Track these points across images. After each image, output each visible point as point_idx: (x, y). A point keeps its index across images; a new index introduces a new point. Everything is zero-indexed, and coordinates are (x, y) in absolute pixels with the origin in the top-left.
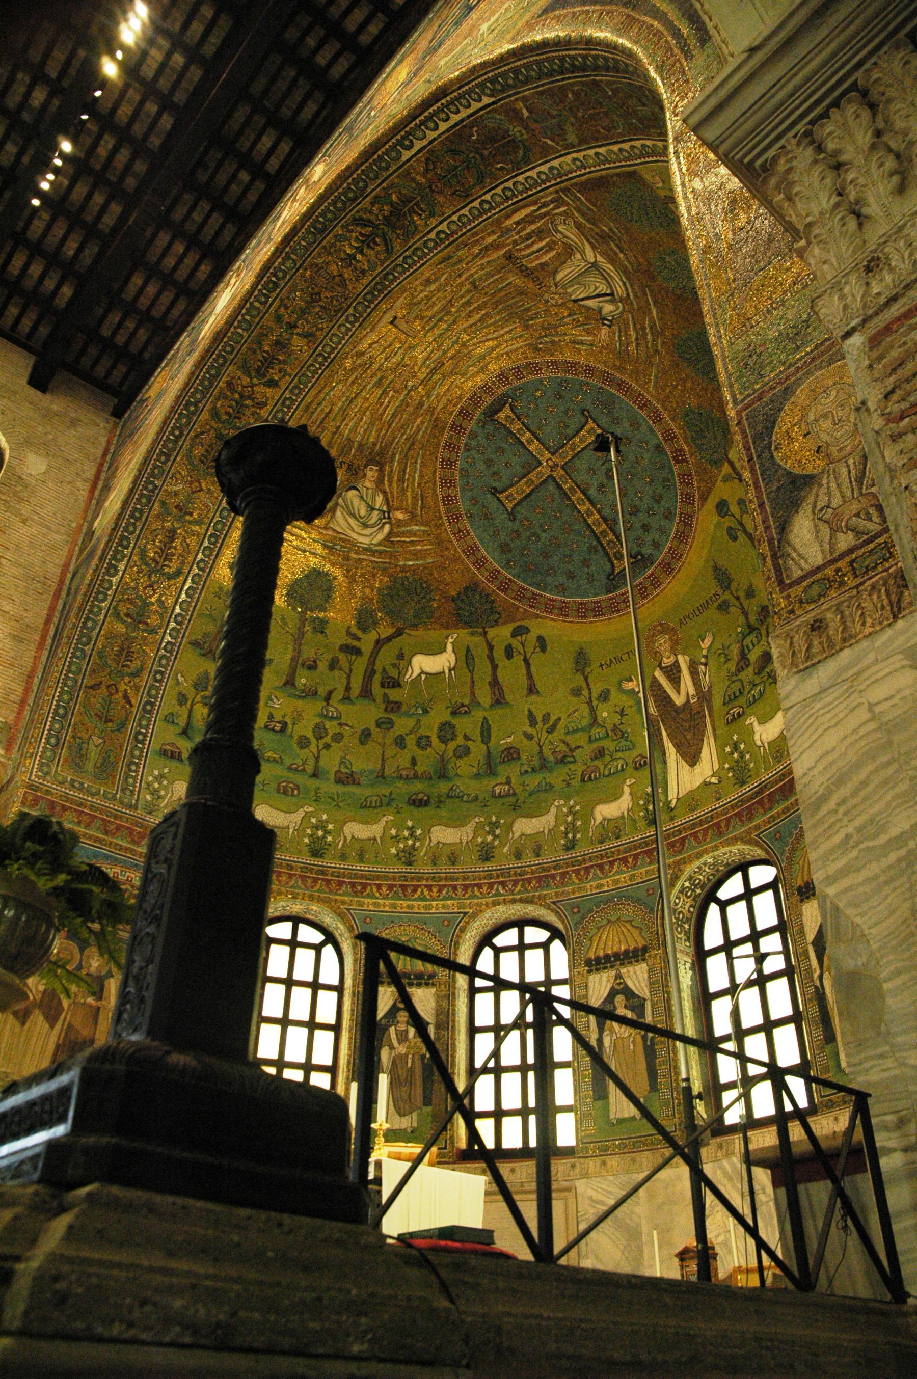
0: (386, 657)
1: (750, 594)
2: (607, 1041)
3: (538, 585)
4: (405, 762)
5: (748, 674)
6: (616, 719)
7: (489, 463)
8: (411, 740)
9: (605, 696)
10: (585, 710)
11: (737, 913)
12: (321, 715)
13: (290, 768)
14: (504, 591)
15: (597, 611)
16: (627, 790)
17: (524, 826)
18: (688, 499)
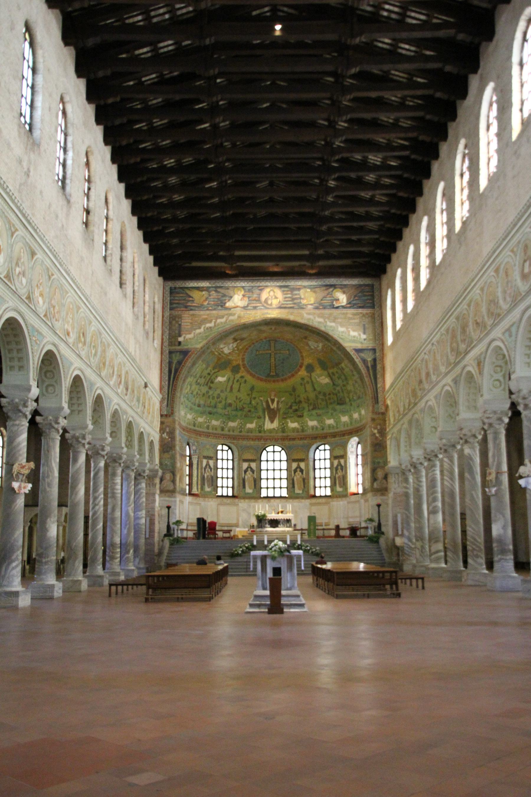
0: (214, 376)
1: (299, 396)
2: (246, 477)
3: (251, 369)
4: (209, 402)
5: (291, 411)
6: (256, 404)
7: (261, 346)
8: (211, 397)
9: (255, 398)
10: (249, 399)
11: (271, 455)
12: (199, 390)
13: (192, 403)
14: (244, 368)
15: (261, 380)
16: (255, 422)
17: (231, 424)
18: (297, 373)
